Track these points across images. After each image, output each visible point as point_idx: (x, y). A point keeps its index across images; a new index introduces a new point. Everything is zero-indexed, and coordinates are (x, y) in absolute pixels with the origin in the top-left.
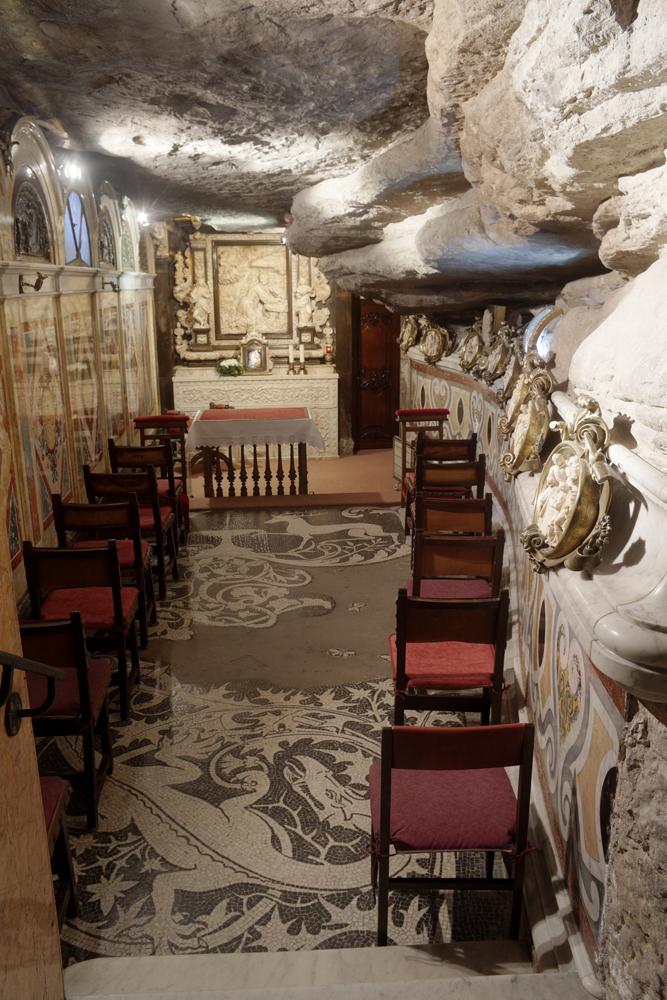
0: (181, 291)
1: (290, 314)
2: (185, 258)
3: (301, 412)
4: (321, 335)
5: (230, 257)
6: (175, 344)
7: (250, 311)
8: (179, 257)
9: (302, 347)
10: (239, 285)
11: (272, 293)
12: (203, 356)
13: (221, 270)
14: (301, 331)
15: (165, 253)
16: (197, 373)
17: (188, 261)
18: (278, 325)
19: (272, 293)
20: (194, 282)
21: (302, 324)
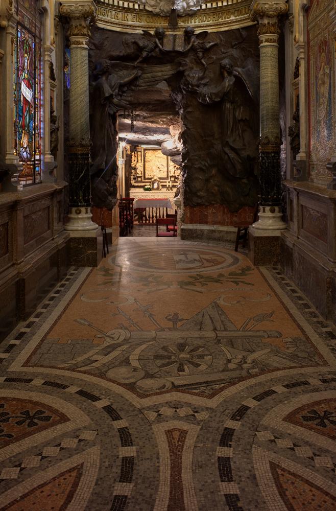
1: (168, 172)
3: (167, 199)
4: (178, 179)
5: (149, 154)
6: (131, 181)
7: (155, 171)
8: (133, 154)
9: (171, 182)
10: (151, 163)
11: (162, 165)
12: (139, 184)
14: (171, 177)
15: (129, 153)
16: (137, 190)
17: (136, 155)
18: (165, 175)
19: (162, 165)
20: (137, 161)
21: (171, 175)
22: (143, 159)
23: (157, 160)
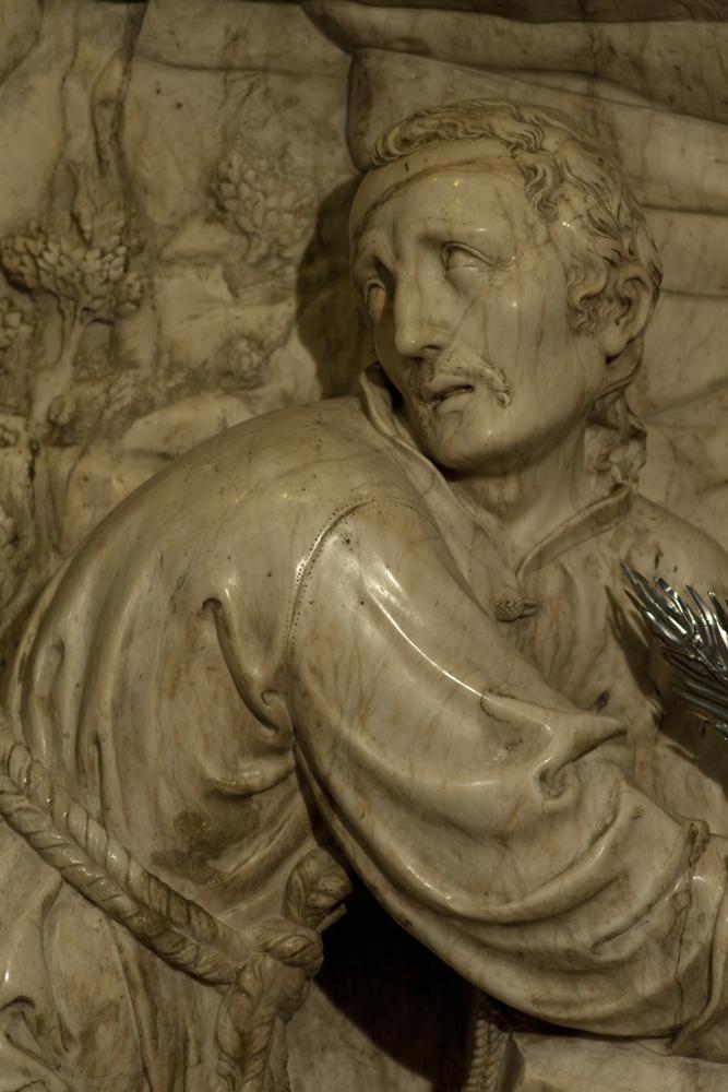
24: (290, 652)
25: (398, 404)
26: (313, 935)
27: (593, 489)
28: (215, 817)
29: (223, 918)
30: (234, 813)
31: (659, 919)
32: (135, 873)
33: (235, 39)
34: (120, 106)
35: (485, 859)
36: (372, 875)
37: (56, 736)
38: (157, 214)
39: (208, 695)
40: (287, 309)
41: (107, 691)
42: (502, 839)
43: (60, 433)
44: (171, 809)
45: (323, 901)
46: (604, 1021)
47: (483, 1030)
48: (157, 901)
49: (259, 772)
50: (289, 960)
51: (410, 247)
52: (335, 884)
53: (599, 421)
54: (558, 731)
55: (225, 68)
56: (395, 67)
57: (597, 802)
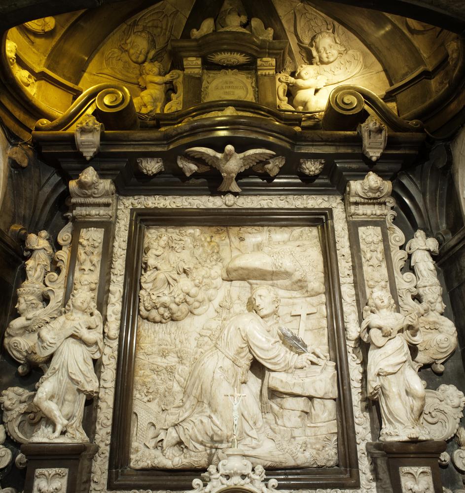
0: (26, 330)
2: (57, 247)
7: (222, 390)
8: (39, 242)
10: (192, 326)
11: (293, 343)
13: (147, 278)
17: (64, 255)
22: (117, 288)
23: (239, 307)
24: (247, 333)
25: (256, 312)
26: (249, 363)
27: (275, 321)
28: (240, 350)
29: (241, 361)
30: (242, 350)
31: (283, 359)
32: (232, 356)
33: (240, 284)
34: (230, 290)
35: (266, 353)
36: (255, 355)
37: (224, 343)
38: (233, 300)
39: (239, 337)
40: (246, 307)
41: (229, 337)
42: (268, 351)
43: (225, 319)
44: (235, 349)
45: (251, 359)
46: (278, 369)
47: (266, 372)
48: (234, 358)
49: (244, 345)
50: (247, 365)
51: (257, 296)
52: (252, 357)
53: (275, 314)
54: (273, 340)
55: (239, 287)
56: (255, 286)
57: (277, 348)
